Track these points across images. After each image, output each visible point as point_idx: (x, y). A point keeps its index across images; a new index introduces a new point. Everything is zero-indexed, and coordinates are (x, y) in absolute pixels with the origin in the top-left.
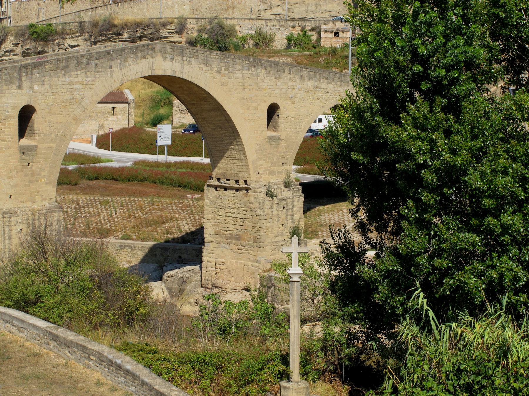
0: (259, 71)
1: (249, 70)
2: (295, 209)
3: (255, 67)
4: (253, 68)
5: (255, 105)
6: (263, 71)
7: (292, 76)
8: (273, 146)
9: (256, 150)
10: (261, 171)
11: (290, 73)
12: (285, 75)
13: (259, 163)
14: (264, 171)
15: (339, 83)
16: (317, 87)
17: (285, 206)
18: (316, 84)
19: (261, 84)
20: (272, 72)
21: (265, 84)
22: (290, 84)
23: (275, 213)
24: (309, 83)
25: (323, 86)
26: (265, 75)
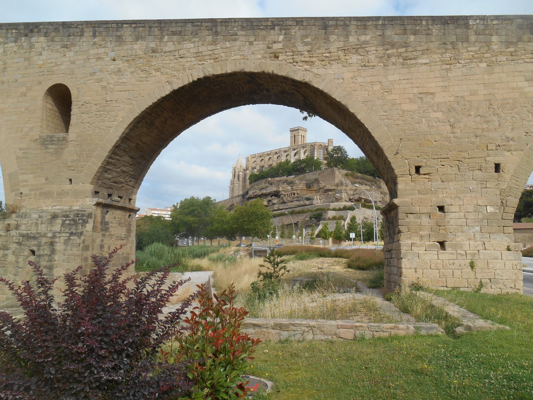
0: (33, 40)
1: (15, 41)
2: (56, 257)
3: (26, 35)
4: (23, 38)
5: (24, 89)
6: (42, 39)
7: (97, 40)
8: (51, 150)
9: (17, 158)
10: (25, 191)
11: (94, 36)
12: (84, 39)
13: (21, 177)
14: (31, 190)
15: (209, 38)
16: (154, 51)
17: (35, 248)
18: (153, 45)
19: (35, 58)
20: (57, 39)
21: (44, 57)
22: (92, 52)
23: (11, 258)
24: (135, 46)
25: (170, 46)
26: (44, 45)
